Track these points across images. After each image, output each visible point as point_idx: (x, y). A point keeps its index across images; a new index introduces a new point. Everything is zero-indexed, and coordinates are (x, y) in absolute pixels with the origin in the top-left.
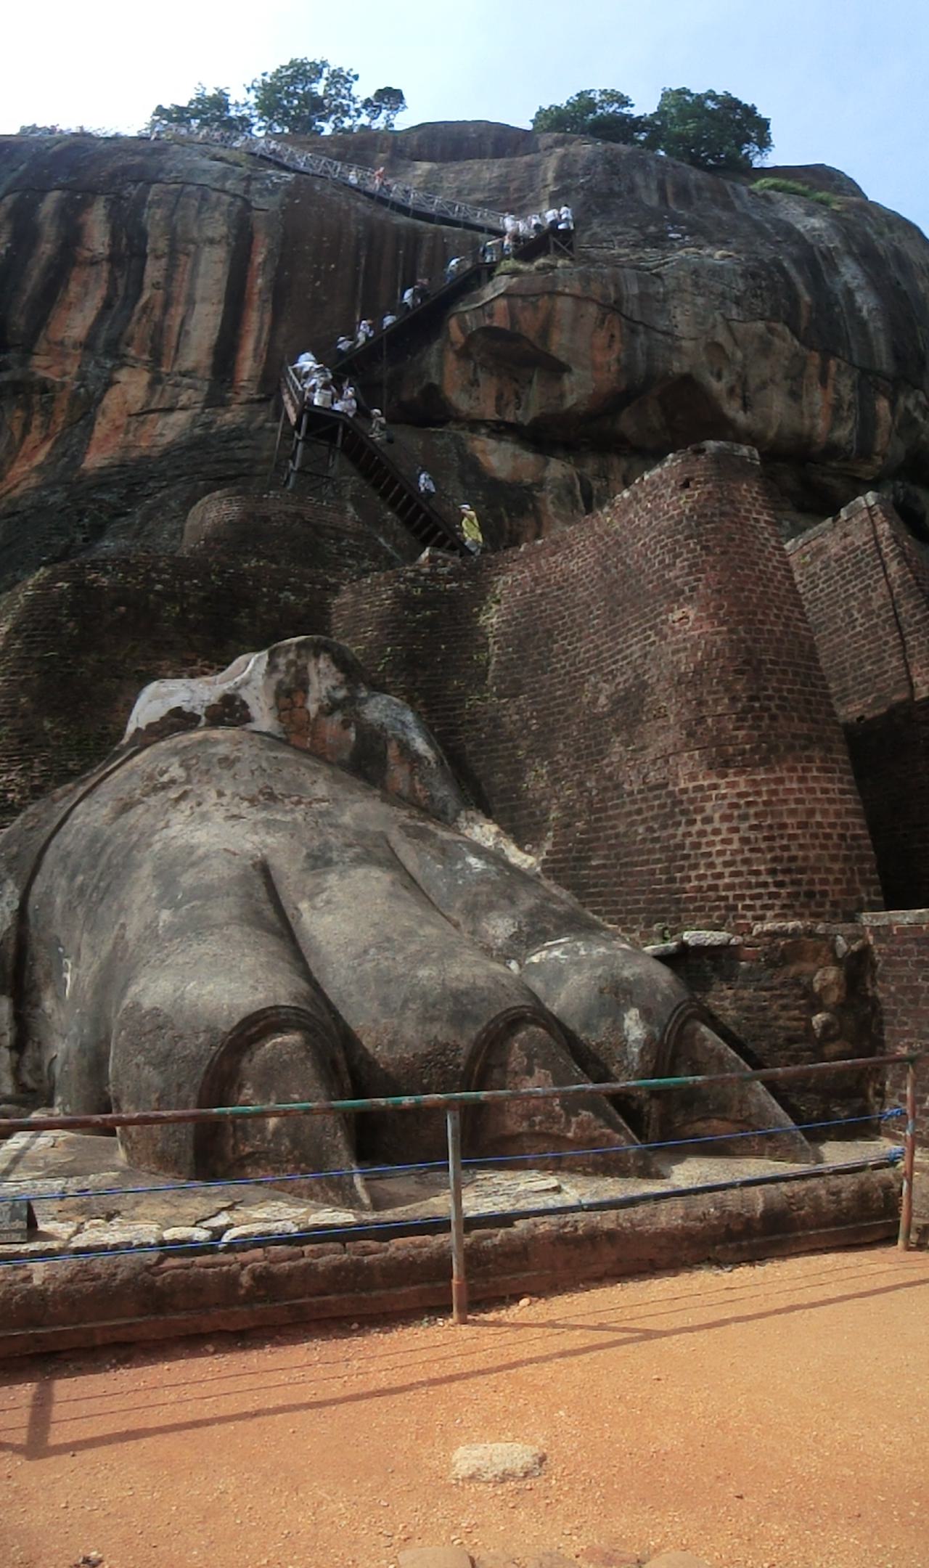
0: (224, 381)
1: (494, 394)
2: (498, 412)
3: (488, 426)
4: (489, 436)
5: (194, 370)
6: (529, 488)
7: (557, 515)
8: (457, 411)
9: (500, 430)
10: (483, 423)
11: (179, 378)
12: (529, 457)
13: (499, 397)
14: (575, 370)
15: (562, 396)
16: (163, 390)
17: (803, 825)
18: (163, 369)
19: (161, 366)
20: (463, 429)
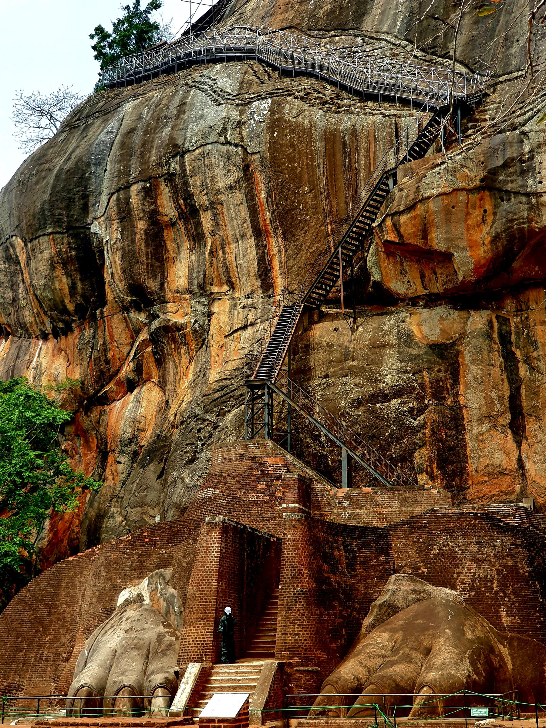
0: (270, 297)
1: (418, 275)
2: (425, 288)
3: (423, 299)
4: (426, 306)
5: (252, 292)
6: (453, 344)
7: (472, 362)
8: (398, 294)
9: (431, 301)
10: (419, 297)
11: (245, 300)
12: (455, 315)
13: (422, 277)
14: (455, 254)
15: (456, 272)
16: (239, 313)
17: (193, 641)
18: (236, 295)
19: (234, 292)
20: (408, 304)
